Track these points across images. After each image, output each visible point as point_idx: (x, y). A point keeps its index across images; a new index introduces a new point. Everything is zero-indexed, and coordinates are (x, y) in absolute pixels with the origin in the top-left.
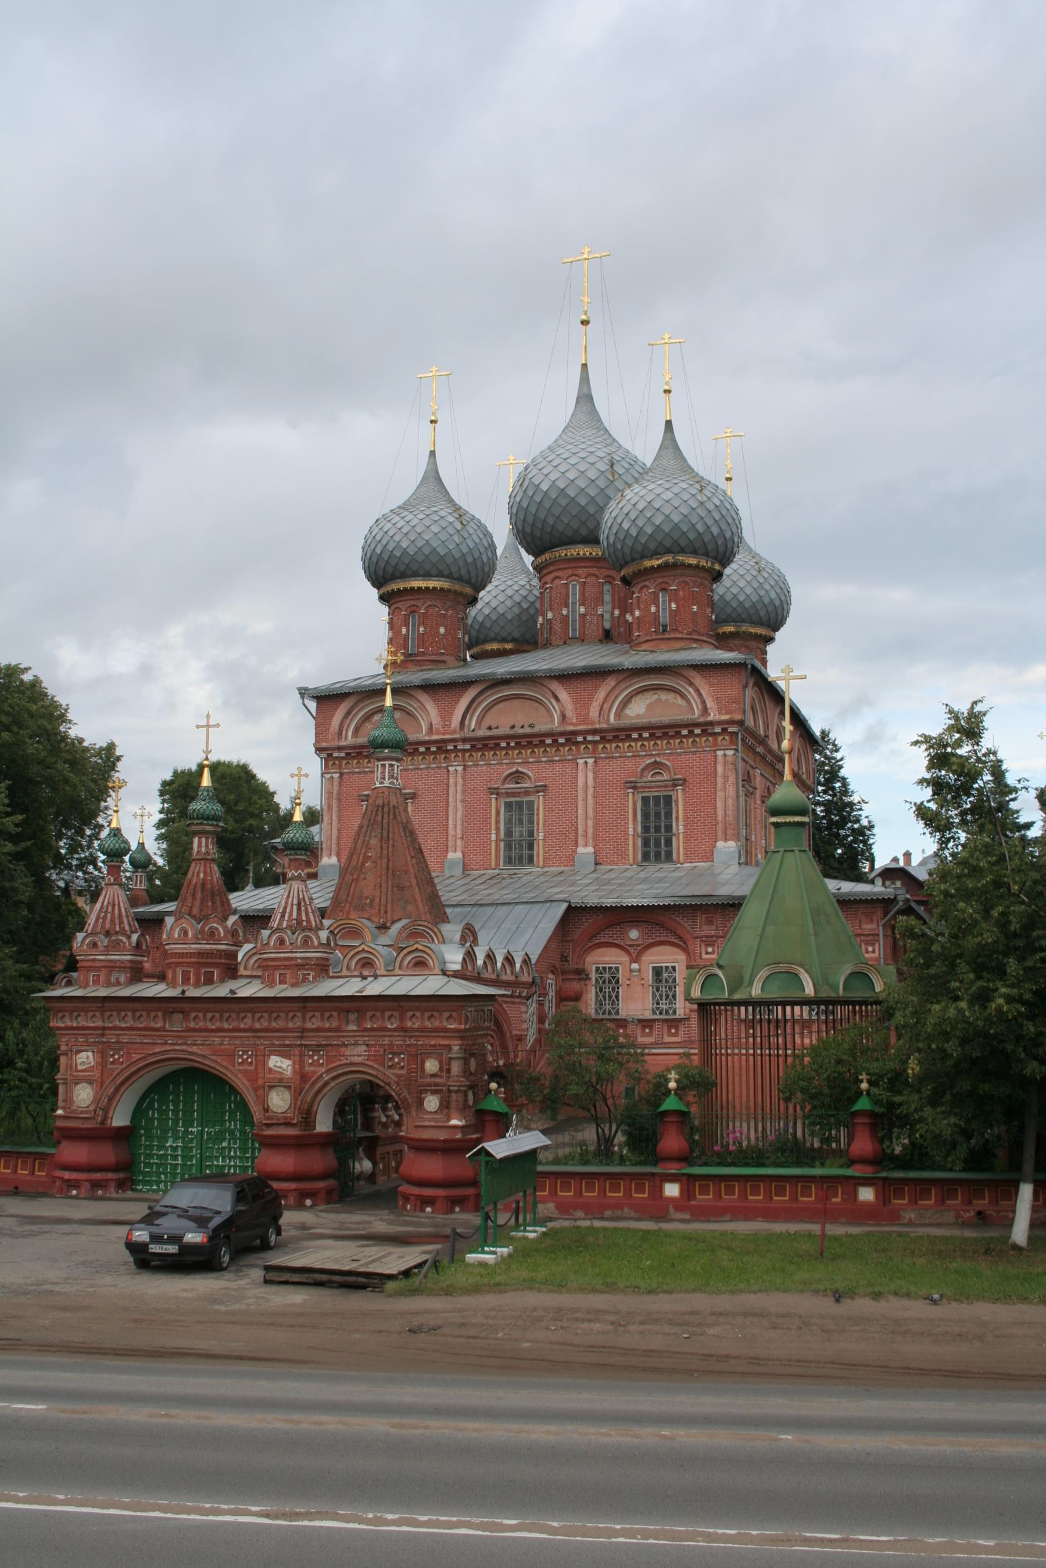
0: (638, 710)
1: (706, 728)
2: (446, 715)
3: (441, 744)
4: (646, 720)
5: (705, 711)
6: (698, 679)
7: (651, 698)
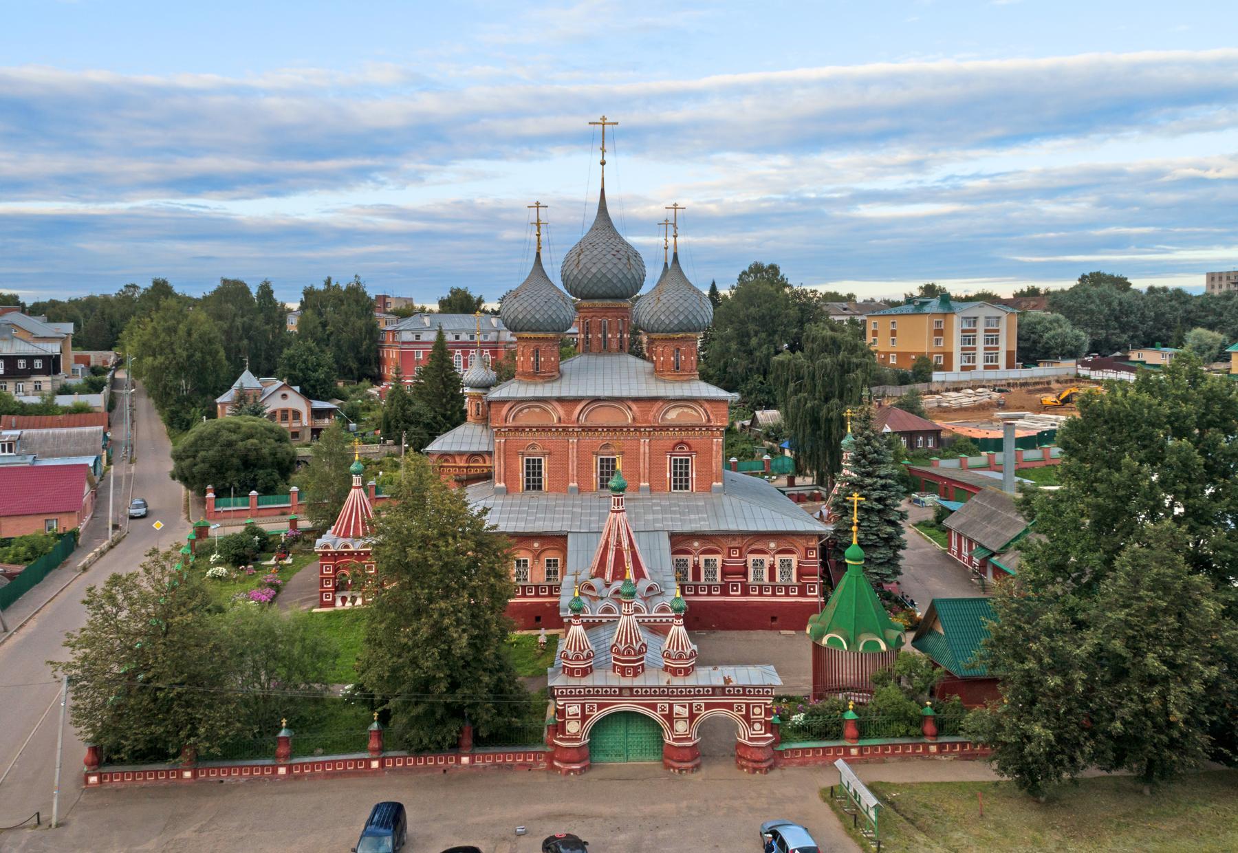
0: (672, 415)
1: (708, 428)
2: (569, 413)
3: (565, 429)
4: (678, 423)
5: (709, 420)
6: (706, 405)
7: (679, 410)
